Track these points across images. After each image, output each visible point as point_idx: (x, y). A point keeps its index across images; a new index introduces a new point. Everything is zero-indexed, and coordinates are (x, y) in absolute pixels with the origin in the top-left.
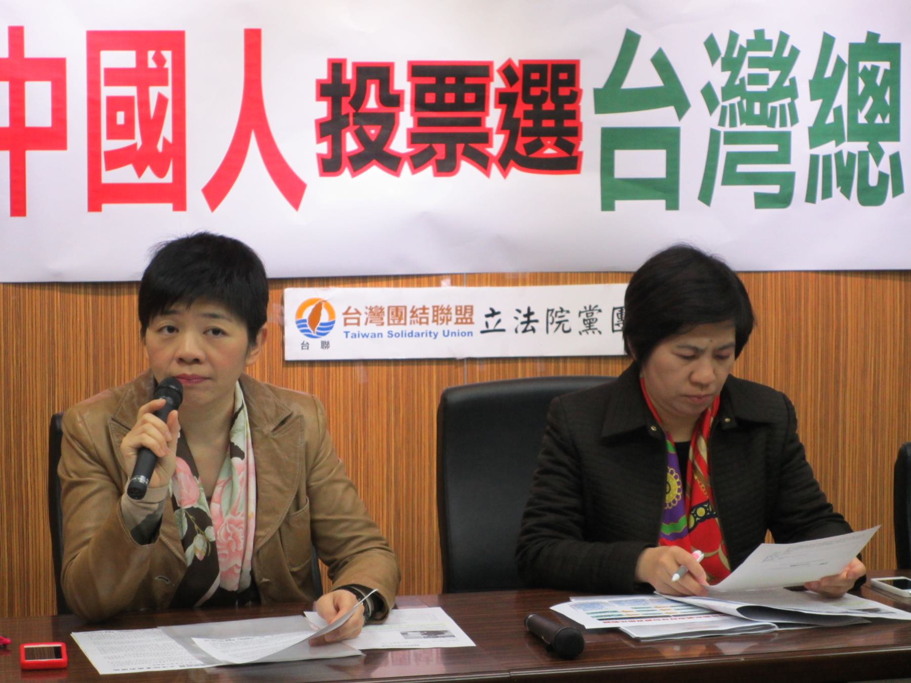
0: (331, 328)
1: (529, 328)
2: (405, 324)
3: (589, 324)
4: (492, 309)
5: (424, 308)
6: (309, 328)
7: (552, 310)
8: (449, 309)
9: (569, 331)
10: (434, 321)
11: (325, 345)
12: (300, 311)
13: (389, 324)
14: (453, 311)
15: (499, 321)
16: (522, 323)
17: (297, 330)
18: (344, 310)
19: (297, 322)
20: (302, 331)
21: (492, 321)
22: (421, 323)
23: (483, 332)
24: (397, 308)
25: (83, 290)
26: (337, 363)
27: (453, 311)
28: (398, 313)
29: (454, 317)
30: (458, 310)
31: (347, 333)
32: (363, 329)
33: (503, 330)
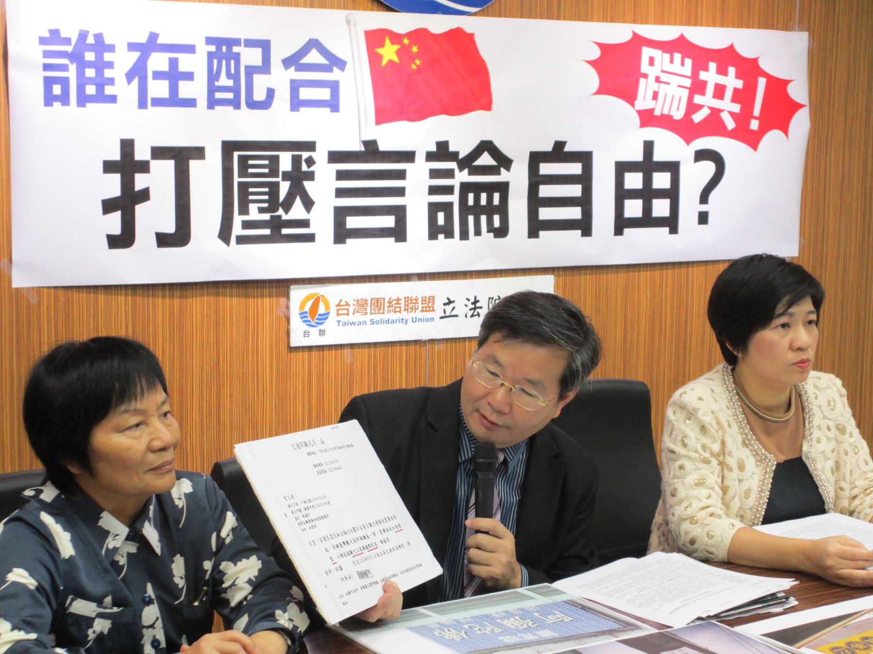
0: (326, 318)
2: (383, 313)
4: (448, 299)
5: (398, 299)
6: (309, 319)
8: (416, 300)
10: (405, 310)
11: (322, 333)
12: (302, 306)
13: (371, 313)
14: (420, 301)
15: (454, 308)
16: (471, 309)
17: (300, 321)
18: (337, 303)
19: (300, 314)
20: (304, 322)
21: (448, 308)
22: (395, 312)
23: (442, 318)
24: (378, 299)
25: (123, 292)
26: (330, 347)
27: (420, 301)
28: (378, 304)
29: (420, 306)
30: (424, 300)
31: (339, 321)
32: (352, 318)
33: (457, 316)
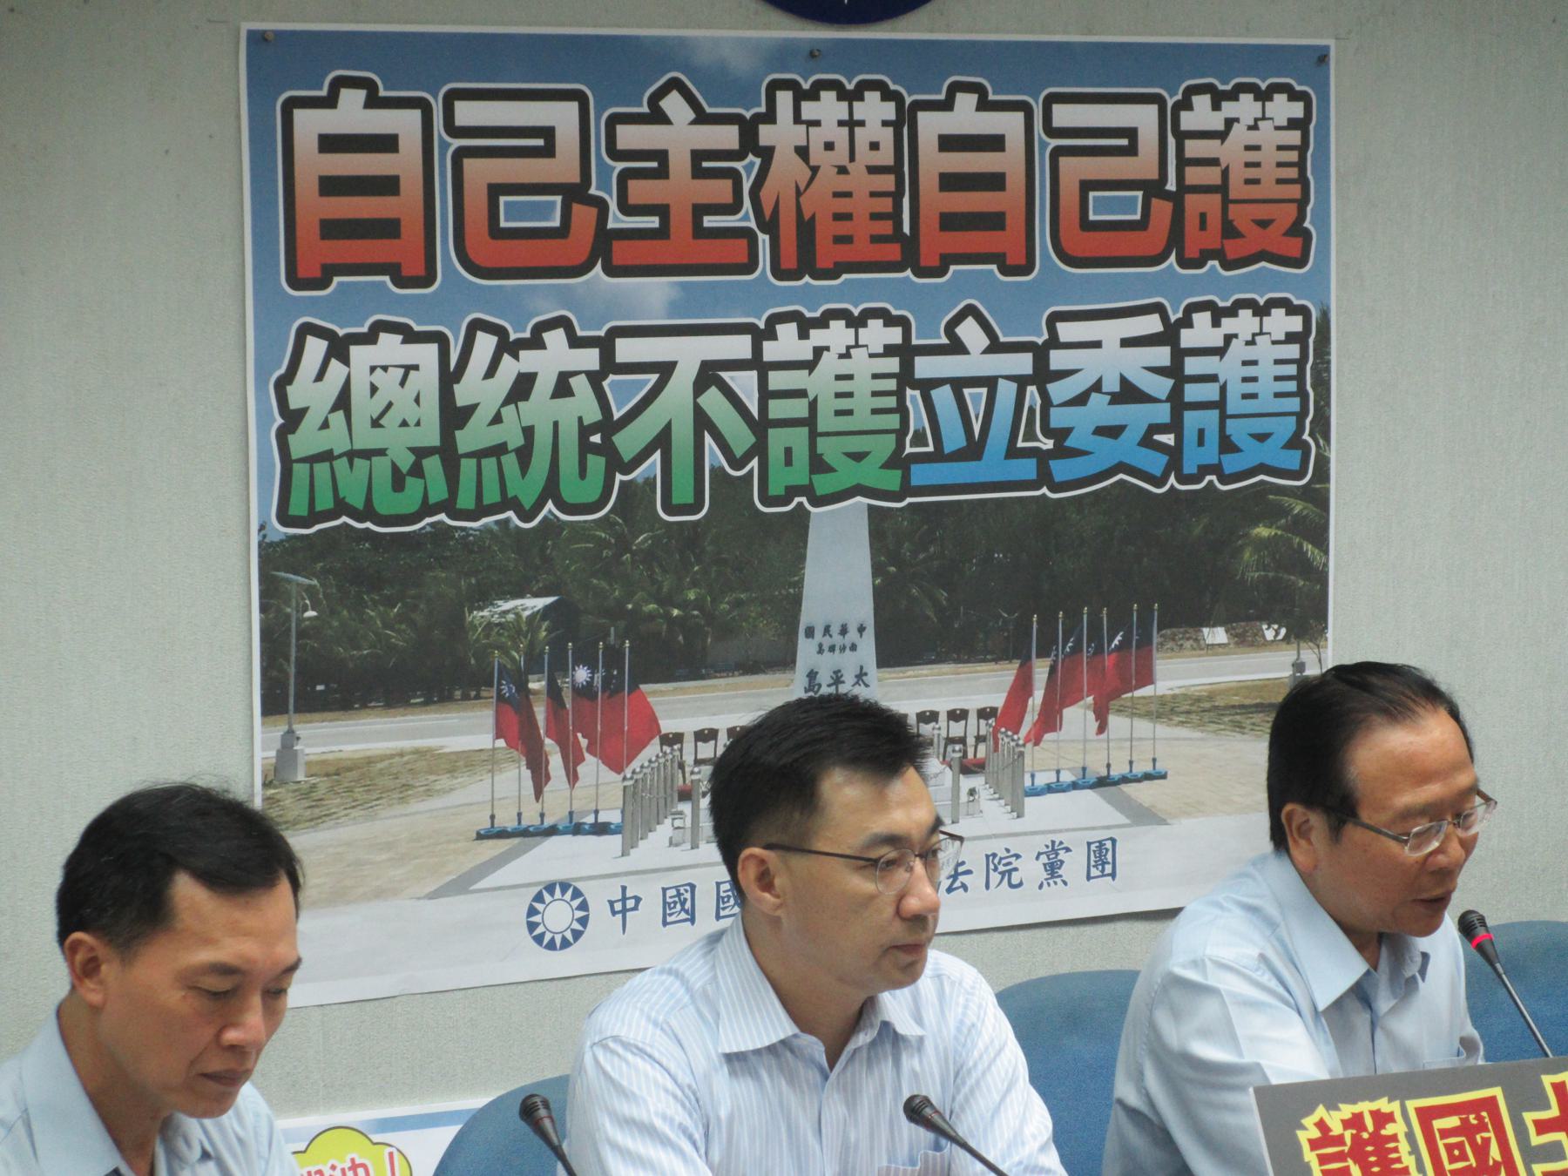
1: (957, 884)
3: (1053, 869)
7: (994, 855)
9: (1020, 884)
